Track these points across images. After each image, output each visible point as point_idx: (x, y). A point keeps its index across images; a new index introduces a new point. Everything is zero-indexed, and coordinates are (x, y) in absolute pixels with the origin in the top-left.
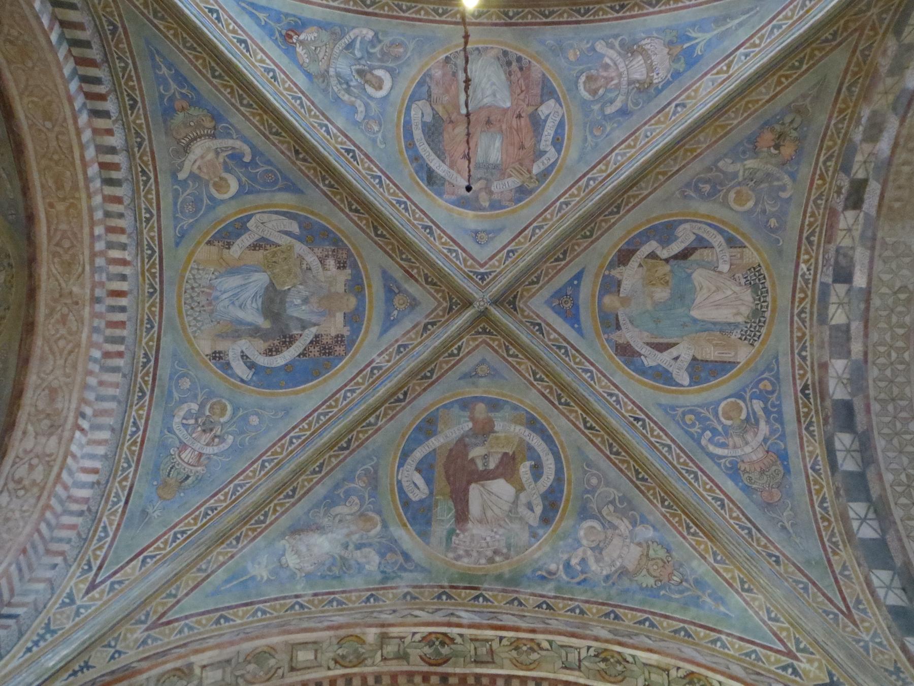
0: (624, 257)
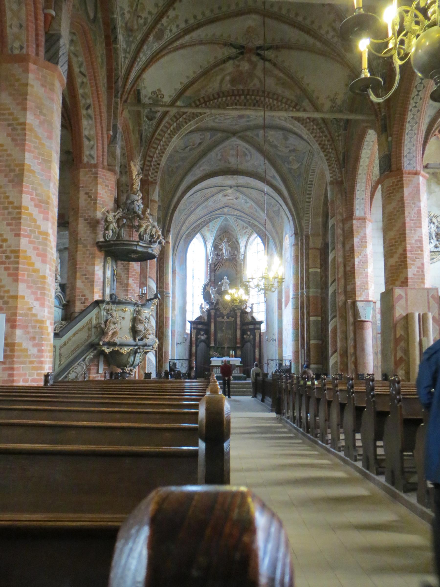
0: (200, 144)
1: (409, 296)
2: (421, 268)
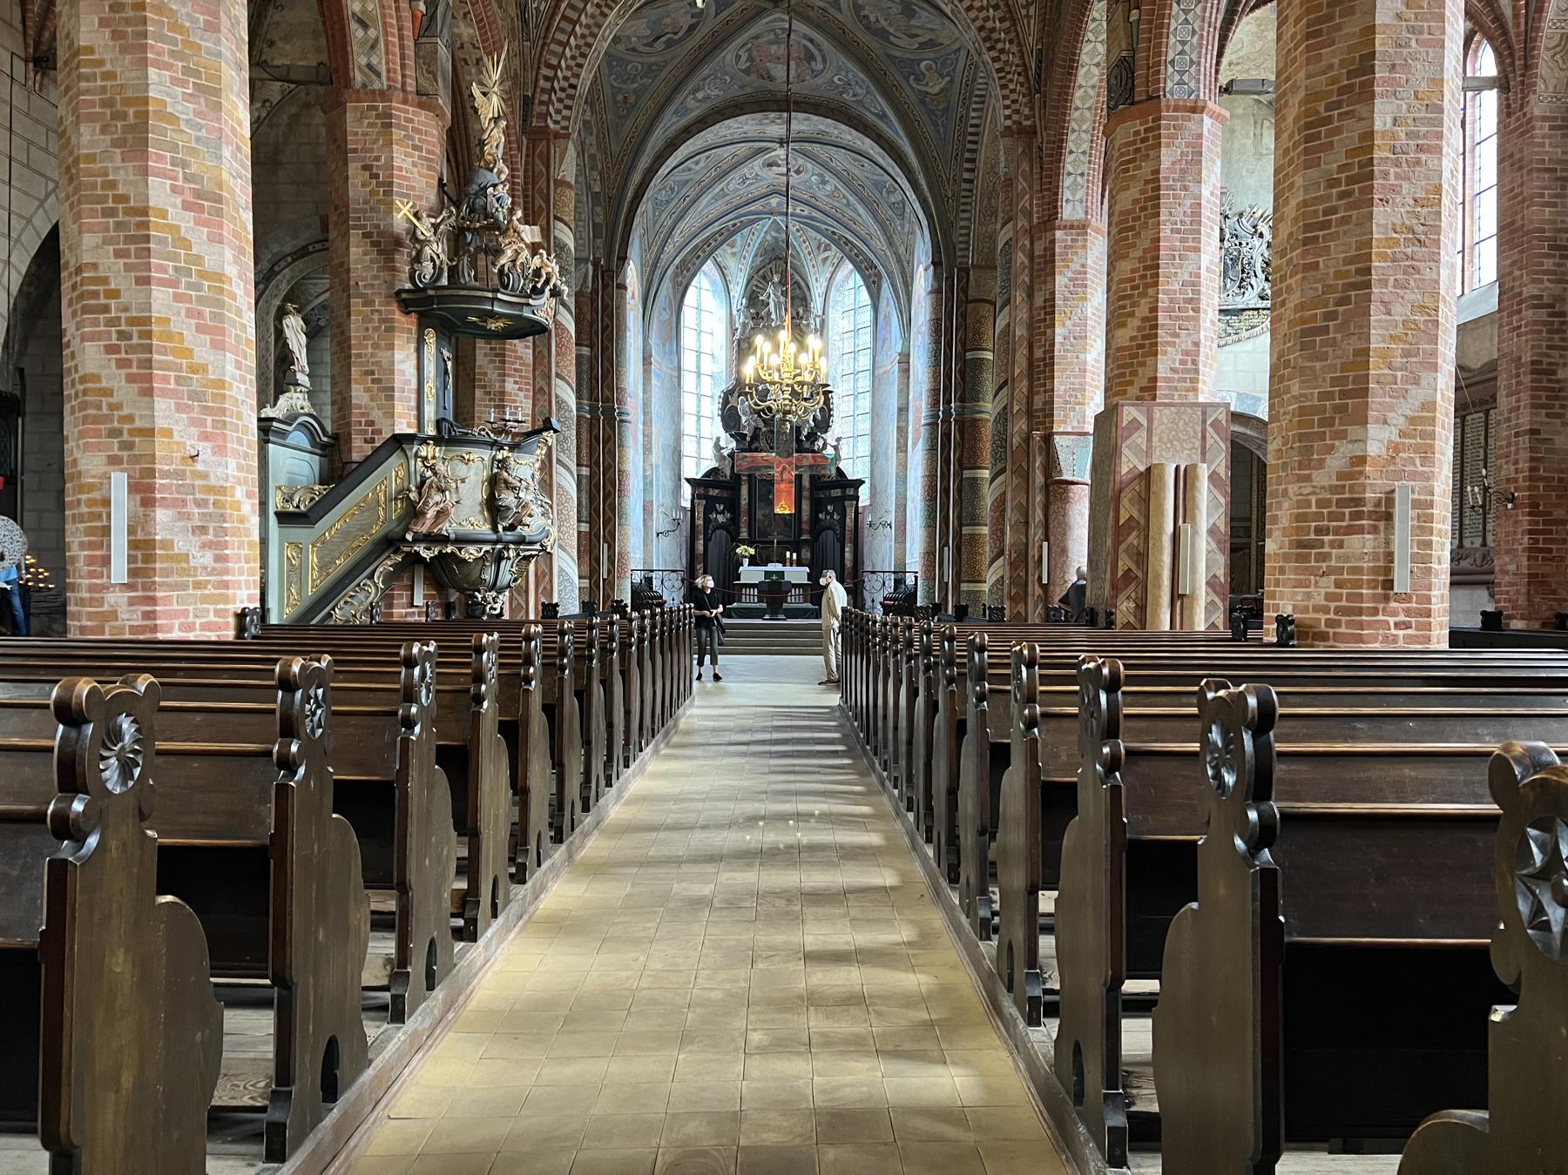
0: (692, 28)
1: (1156, 423)
2: (1192, 355)
